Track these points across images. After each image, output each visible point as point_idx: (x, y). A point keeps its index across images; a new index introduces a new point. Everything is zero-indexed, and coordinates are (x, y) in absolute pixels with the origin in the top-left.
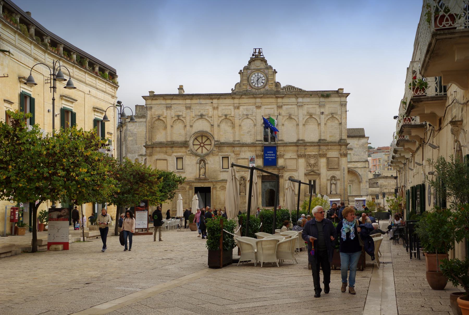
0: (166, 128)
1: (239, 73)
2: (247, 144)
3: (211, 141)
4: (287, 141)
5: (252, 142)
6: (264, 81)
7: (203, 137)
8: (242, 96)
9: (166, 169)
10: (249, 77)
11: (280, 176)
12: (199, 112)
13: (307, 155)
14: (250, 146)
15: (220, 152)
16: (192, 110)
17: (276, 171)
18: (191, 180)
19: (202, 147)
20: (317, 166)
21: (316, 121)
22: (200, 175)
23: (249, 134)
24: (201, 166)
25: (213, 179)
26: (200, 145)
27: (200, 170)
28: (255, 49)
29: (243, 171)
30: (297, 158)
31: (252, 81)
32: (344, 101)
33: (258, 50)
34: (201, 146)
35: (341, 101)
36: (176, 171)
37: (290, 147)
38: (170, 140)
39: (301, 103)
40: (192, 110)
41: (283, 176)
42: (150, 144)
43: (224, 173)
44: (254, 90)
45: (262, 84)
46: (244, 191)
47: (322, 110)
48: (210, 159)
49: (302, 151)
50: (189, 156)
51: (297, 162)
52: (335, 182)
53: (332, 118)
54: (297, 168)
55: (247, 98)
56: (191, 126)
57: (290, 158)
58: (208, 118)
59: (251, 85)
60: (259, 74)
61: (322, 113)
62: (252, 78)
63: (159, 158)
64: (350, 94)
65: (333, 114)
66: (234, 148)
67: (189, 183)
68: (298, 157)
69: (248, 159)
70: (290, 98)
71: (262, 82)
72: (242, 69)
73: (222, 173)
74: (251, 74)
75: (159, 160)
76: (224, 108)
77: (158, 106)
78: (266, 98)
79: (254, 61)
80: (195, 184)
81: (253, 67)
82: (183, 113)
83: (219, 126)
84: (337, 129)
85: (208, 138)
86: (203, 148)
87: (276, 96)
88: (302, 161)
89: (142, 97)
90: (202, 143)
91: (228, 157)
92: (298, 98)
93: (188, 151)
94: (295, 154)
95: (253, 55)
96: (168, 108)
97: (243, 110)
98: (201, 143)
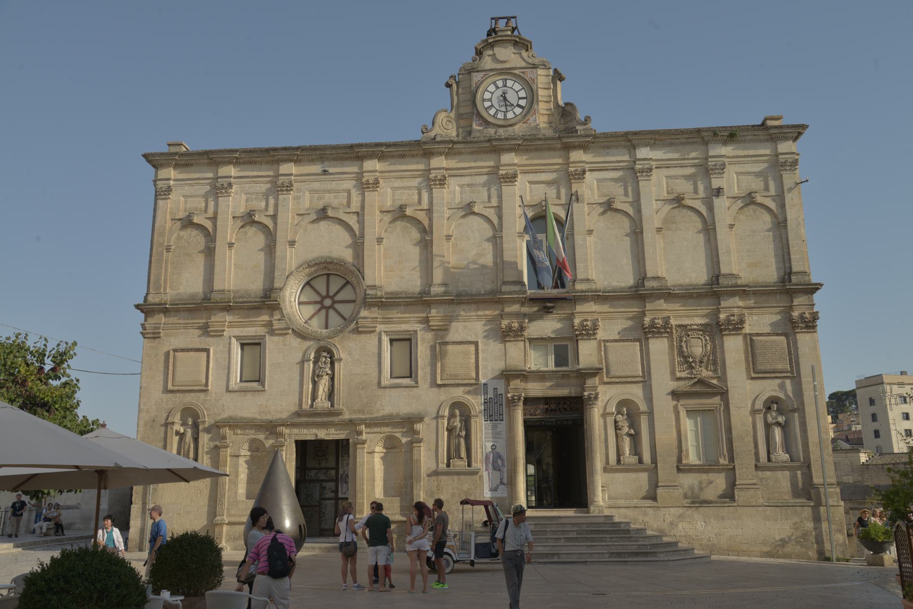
0: (209, 252)
1: (448, 85)
2: (472, 295)
3: (354, 288)
4: (606, 283)
5: (489, 287)
6: (523, 103)
7: (331, 277)
8: (455, 146)
9: (204, 381)
10: (477, 90)
11: (589, 398)
12: (320, 199)
13: (677, 326)
14: (484, 302)
15: (383, 323)
16: (296, 194)
18: (284, 416)
19: (327, 308)
20: (715, 363)
22: (314, 398)
24: (317, 366)
25: (359, 412)
26: (321, 302)
27: (315, 383)
28: (496, 19)
29: (458, 385)
30: (643, 337)
31: (487, 104)
32: (788, 151)
33: (506, 20)
34: (323, 307)
35: (780, 151)
36: (236, 388)
38: (221, 288)
39: (646, 162)
40: (296, 194)
41: (596, 398)
42: (157, 300)
43: (393, 390)
44: (491, 131)
45: (518, 111)
46: (463, 454)
47: (716, 183)
49: (658, 310)
50: (281, 338)
51: (641, 350)
52: (781, 419)
53: (752, 207)
54: (643, 371)
55: (472, 153)
56: (292, 243)
58: (345, 218)
59: (484, 114)
60: (510, 83)
61: (718, 192)
62: (487, 96)
63: (183, 346)
64: (804, 127)
65: (756, 192)
66: (428, 309)
70: (609, 147)
71: (519, 106)
72: (456, 73)
73: (388, 389)
74: (482, 82)
75: (183, 350)
76: (398, 183)
77: (191, 185)
78: (531, 151)
79: (491, 46)
80: (296, 431)
81: (487, 62)
82: (267, 205)
83: (380, 240)
85: (348, 282)
86: (331, 312)
87: (565, 140)
88: (659, 347)
89: (145, 156)
90: (328, 296)
91: (410, 340)
92: (635, 148)
93: (279, 320)
95: (489, 35)
96: (223, 188)
97: (457, 188)
98: (323, 298)
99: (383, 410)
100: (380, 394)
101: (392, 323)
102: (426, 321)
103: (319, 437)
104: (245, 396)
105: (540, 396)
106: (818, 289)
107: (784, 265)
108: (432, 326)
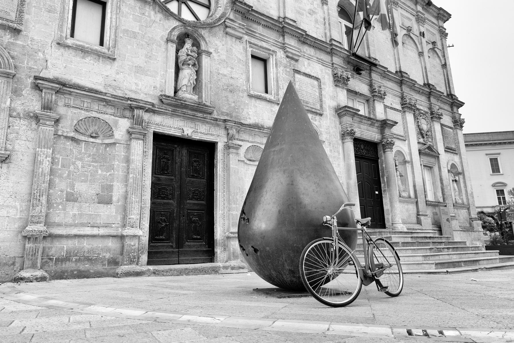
9: (13, 16)
17: (375, 130)
21: (415, 47)
23: (313, 18)
37: (388, 82)
47: (422, 30)
48: (216, 42)
57: (391, 106)
67: (131, 108)
68: (403, 108)
69: (317, 79)
73: (253, 100)
80: (157, 119)
84: (441, 74)
91: (265, 61)
94: (398, 100)
99: (250, 118)
100: (247, 102)
101: (254, 37)
102: (283, 47)
103: (185, 133)
104: (83, 58)
105: (359, 136)
106: (462, 106)
107: (446, 89)
108: (289, 52)
